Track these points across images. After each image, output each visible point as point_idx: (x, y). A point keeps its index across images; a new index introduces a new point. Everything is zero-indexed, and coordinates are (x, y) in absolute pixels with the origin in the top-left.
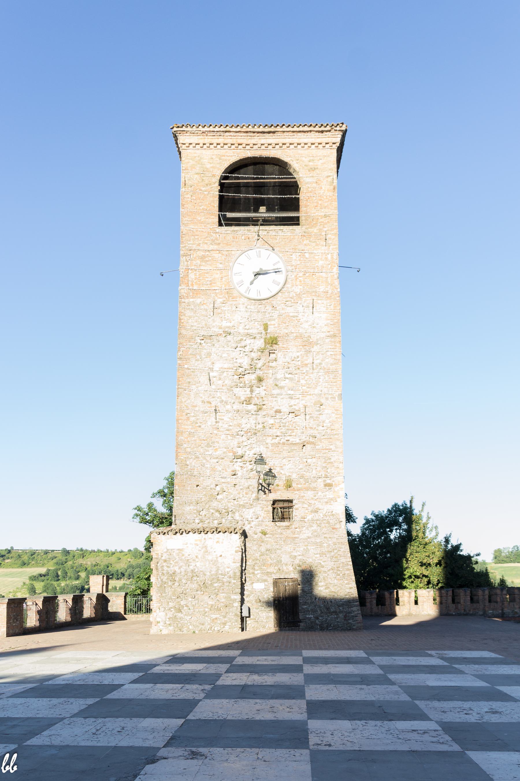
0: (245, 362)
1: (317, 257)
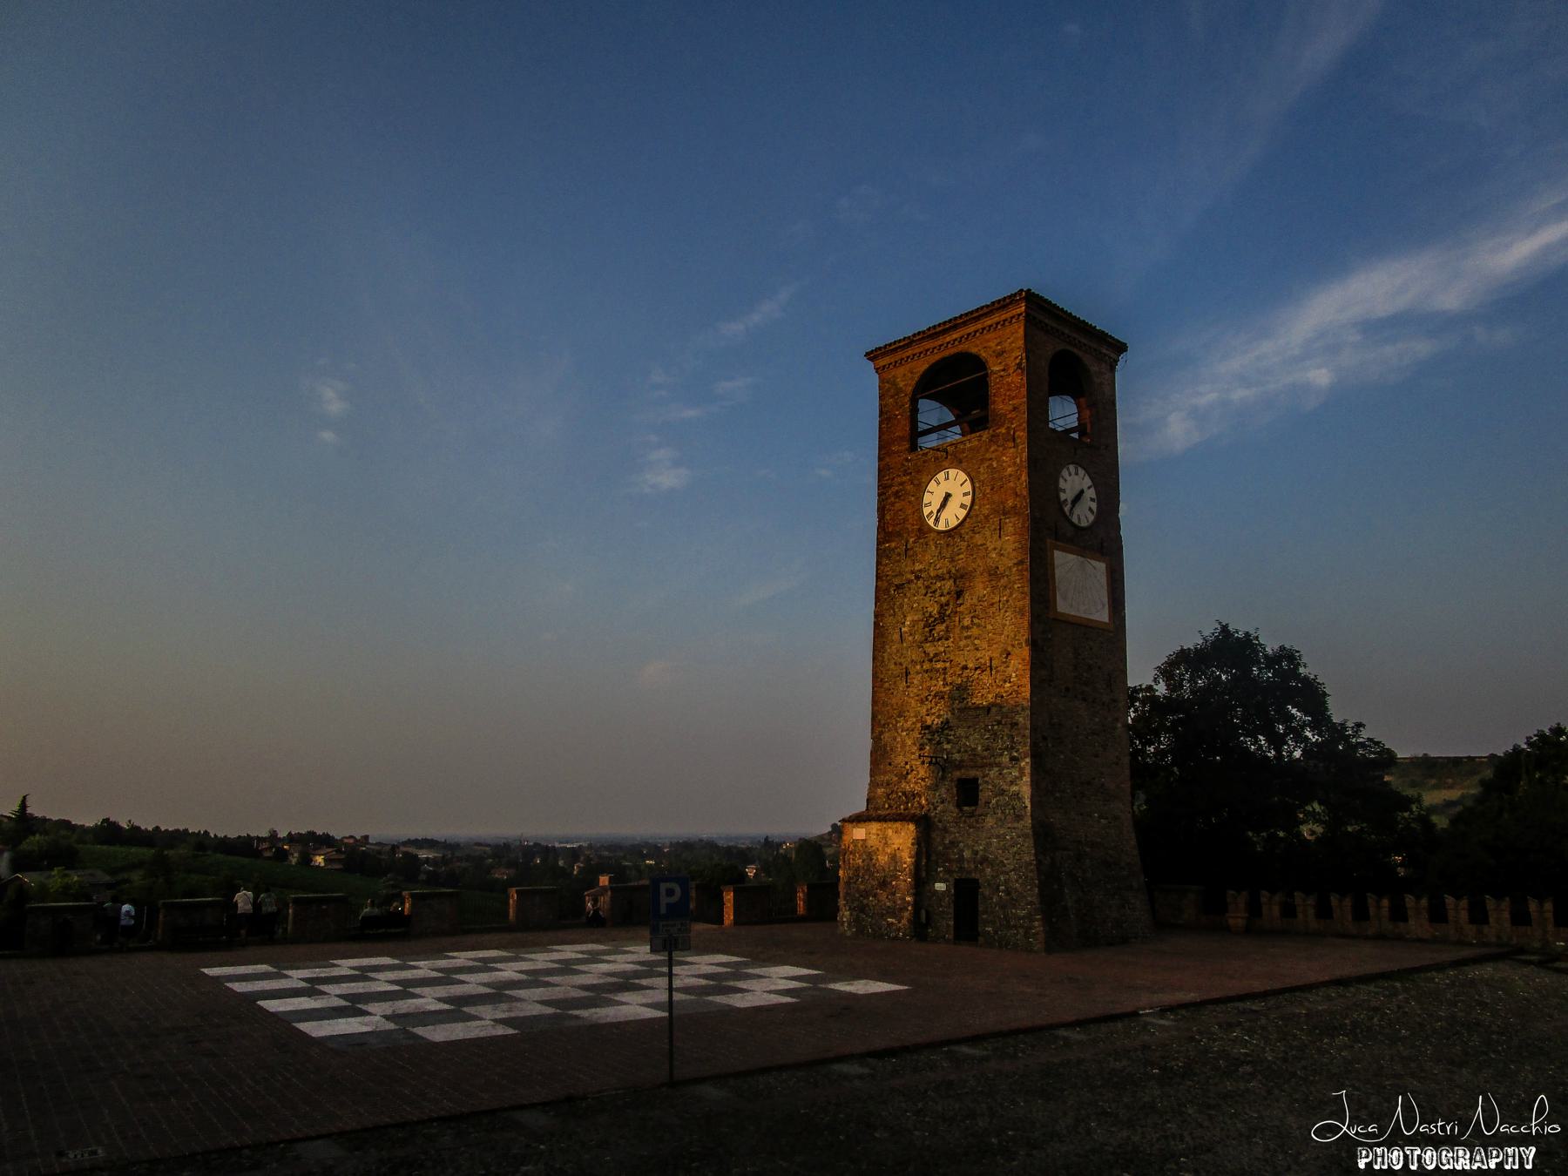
0: (935, 610)
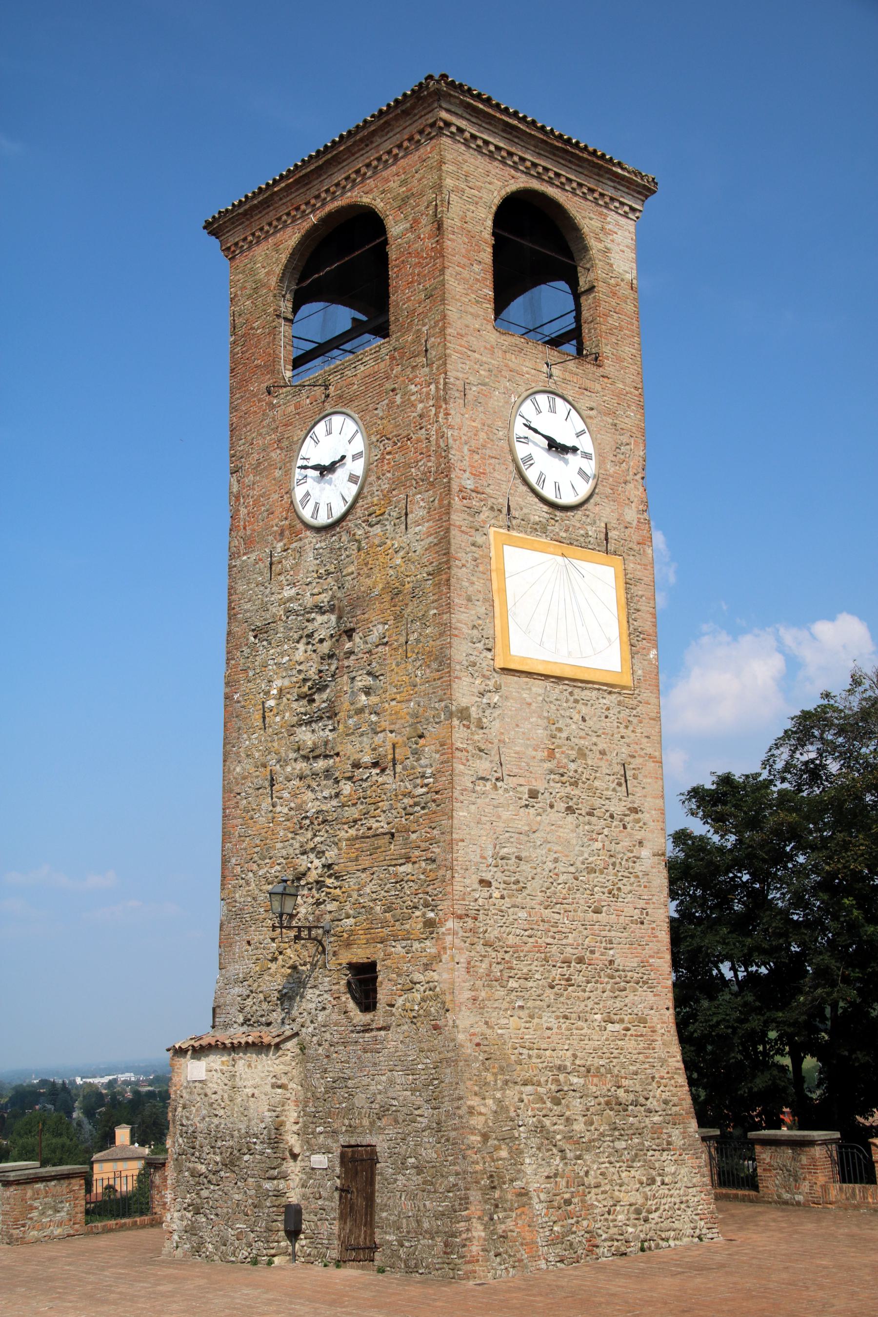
1: (413, 398)
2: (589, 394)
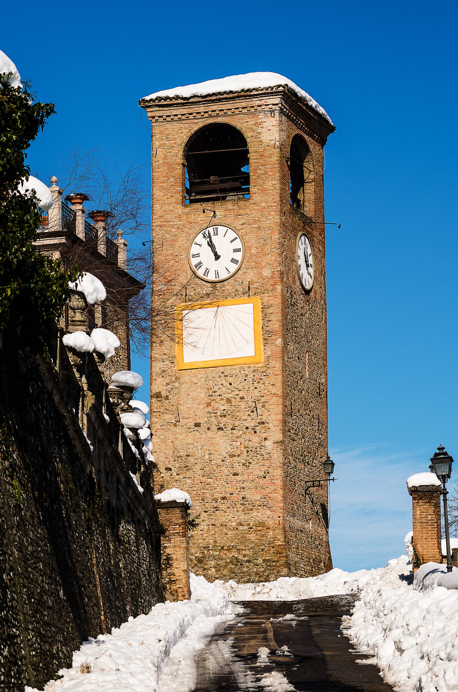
2: (241, 217)
